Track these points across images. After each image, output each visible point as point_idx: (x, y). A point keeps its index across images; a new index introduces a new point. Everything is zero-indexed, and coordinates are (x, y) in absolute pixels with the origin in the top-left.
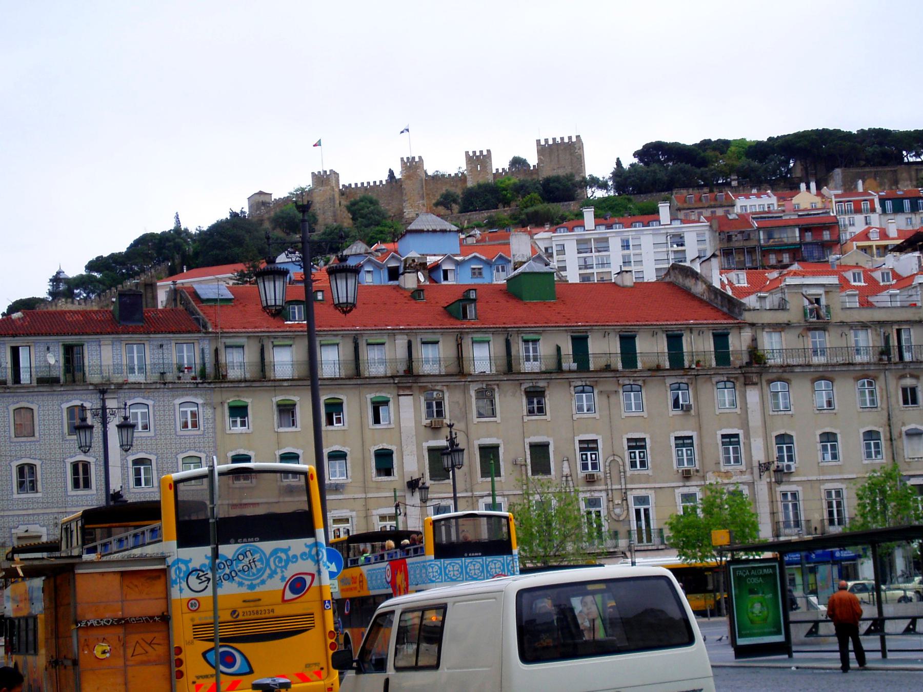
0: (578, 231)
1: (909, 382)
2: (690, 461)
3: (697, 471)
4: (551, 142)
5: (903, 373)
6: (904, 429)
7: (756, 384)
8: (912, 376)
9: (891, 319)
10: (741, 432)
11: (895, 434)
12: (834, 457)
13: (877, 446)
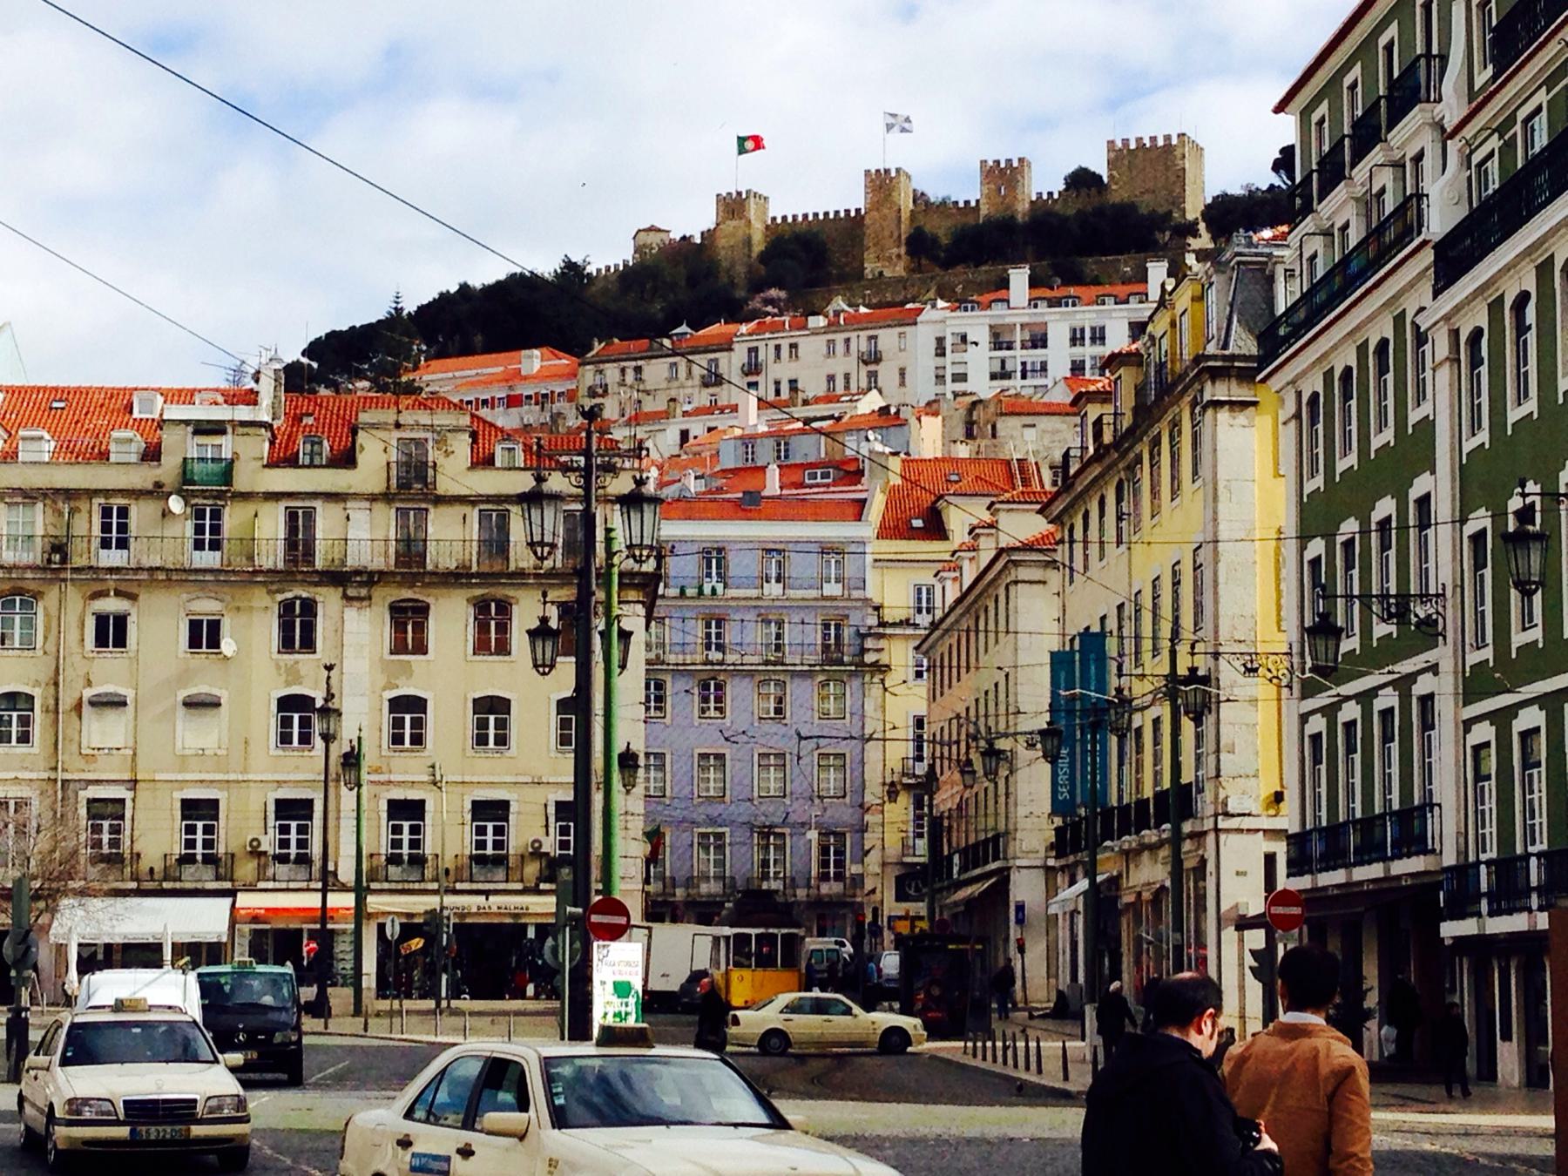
0: (998, 310)
1: (111, 605)
4: (1133, 146)
5: (97, 587)
6: (88, 693)
8: (118, 593)
9: (94, 486)
13: (25, 722)
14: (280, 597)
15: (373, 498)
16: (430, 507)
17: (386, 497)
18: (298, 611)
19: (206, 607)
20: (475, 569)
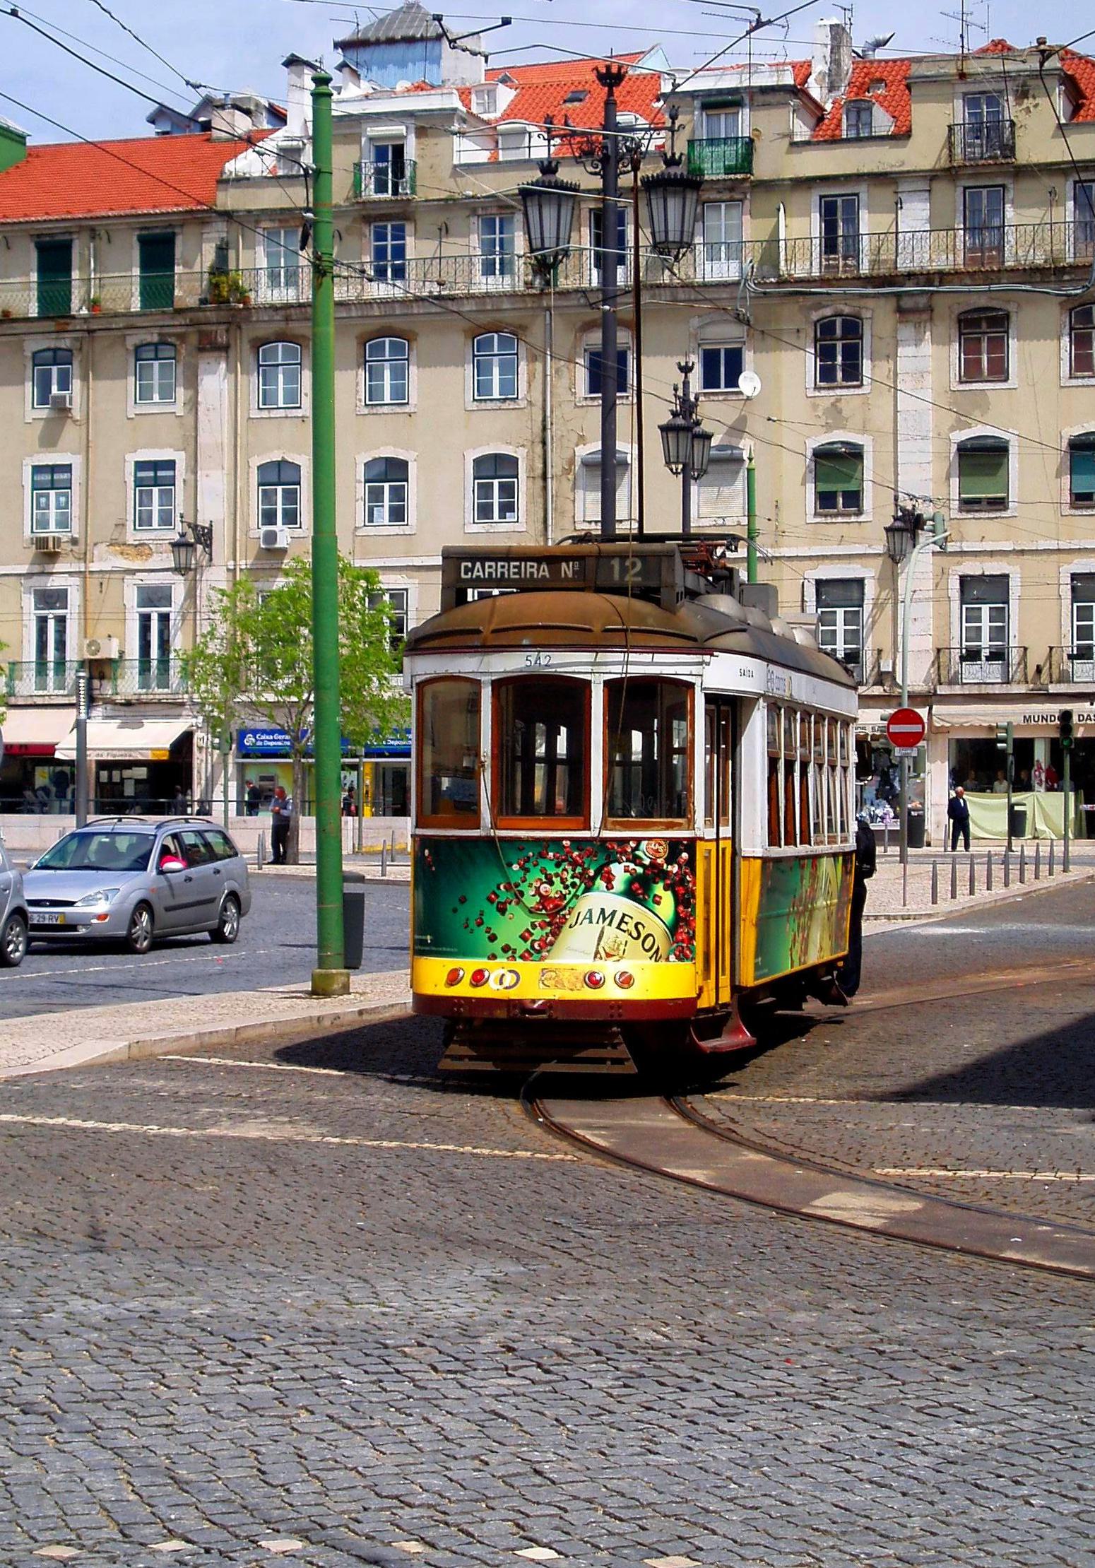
2: (64, 523)
3: (74, 541)
7: (226, 348)
10: (180, 458)
11: (556, 462)
12: (398, 514)
13: (508, 490)
14: (815, 316)
15: (932, 176)
16: (1009, 183)
17: (949, 173)
18: (839, 332)
19: (724, 333)
20: (1070, 260)
